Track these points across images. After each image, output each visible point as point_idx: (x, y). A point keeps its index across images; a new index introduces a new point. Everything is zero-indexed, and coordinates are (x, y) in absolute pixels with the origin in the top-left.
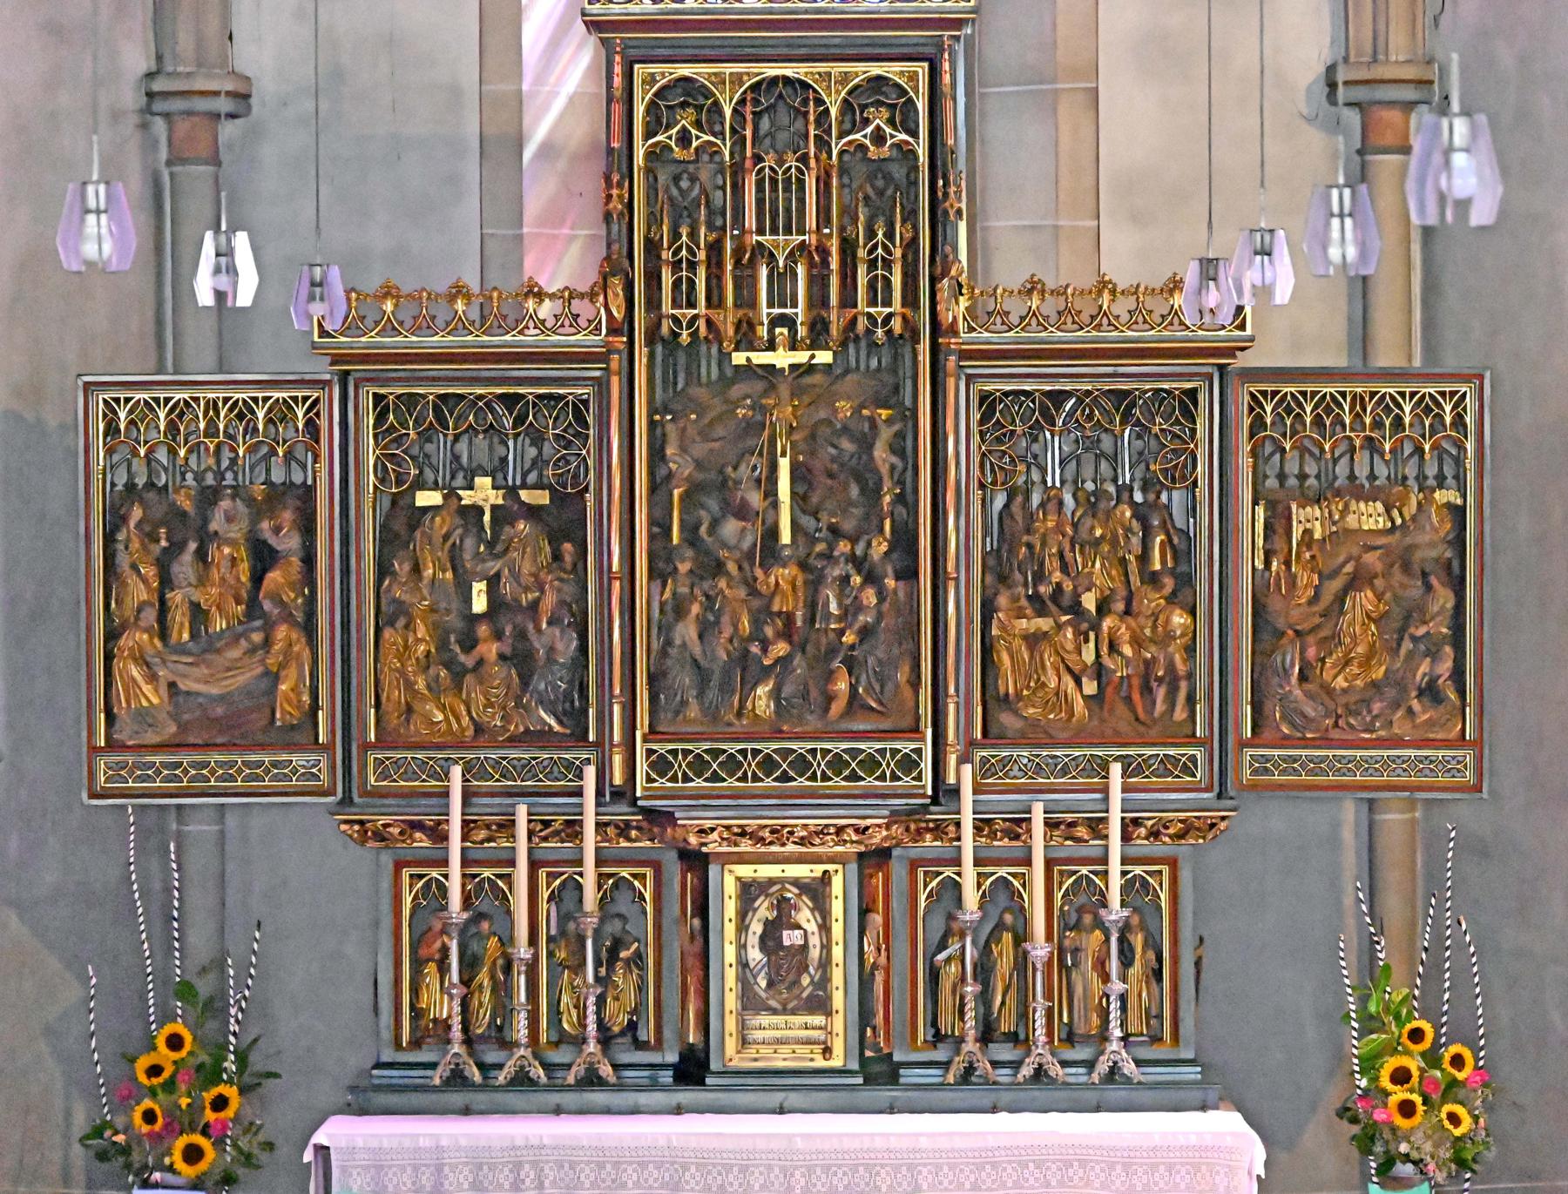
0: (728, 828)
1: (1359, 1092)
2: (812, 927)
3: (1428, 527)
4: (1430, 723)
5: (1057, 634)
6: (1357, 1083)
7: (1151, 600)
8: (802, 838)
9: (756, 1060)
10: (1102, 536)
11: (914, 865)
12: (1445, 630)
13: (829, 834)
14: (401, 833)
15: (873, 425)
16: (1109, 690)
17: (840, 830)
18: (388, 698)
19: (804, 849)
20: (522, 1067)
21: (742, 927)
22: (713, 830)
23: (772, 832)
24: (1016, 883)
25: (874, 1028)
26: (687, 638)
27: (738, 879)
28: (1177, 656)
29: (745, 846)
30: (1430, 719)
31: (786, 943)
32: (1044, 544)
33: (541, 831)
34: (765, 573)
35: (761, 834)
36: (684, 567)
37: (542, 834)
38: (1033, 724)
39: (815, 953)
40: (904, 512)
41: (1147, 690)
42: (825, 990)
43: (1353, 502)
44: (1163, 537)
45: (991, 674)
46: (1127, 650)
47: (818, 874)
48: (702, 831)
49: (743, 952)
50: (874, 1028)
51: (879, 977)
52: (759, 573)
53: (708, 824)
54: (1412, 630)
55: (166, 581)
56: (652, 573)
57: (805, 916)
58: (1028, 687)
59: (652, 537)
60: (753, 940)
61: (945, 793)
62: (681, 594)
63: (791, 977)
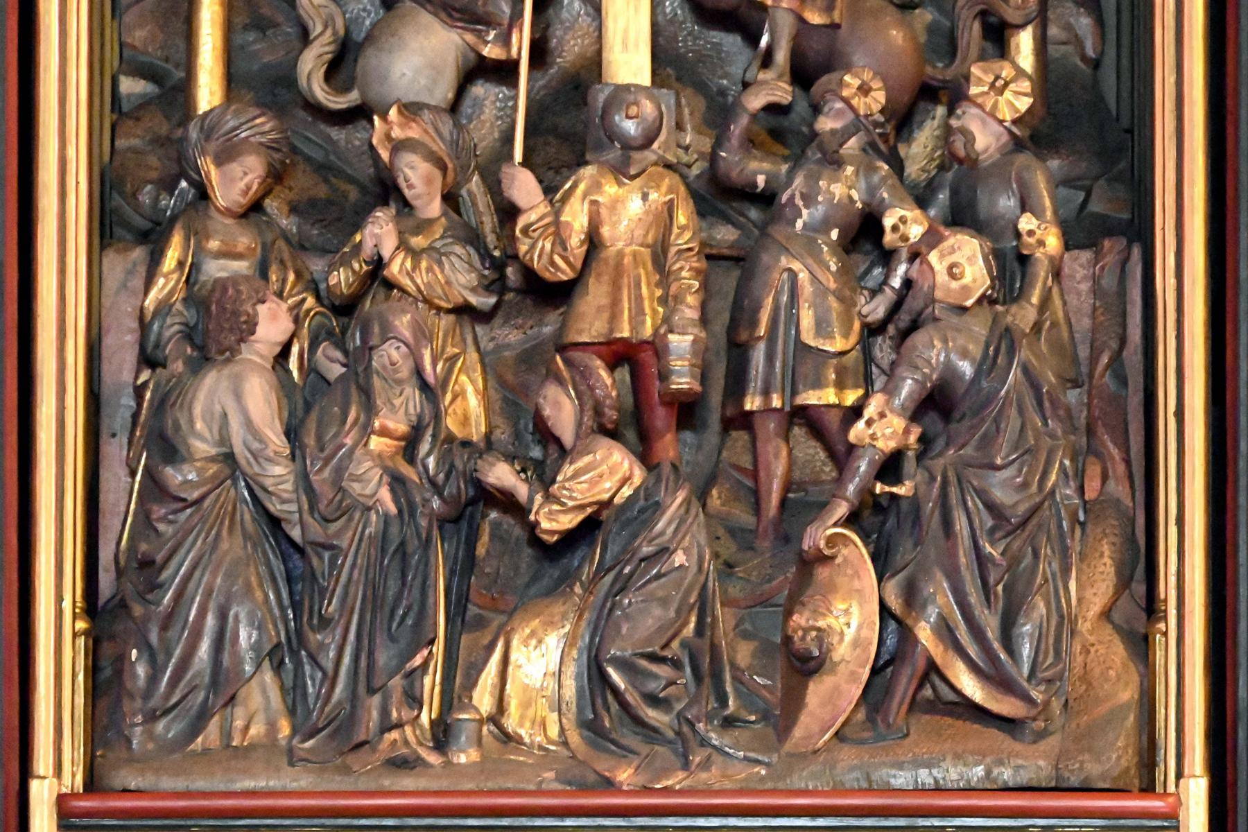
34: (549, 190)
62: (221, 285)
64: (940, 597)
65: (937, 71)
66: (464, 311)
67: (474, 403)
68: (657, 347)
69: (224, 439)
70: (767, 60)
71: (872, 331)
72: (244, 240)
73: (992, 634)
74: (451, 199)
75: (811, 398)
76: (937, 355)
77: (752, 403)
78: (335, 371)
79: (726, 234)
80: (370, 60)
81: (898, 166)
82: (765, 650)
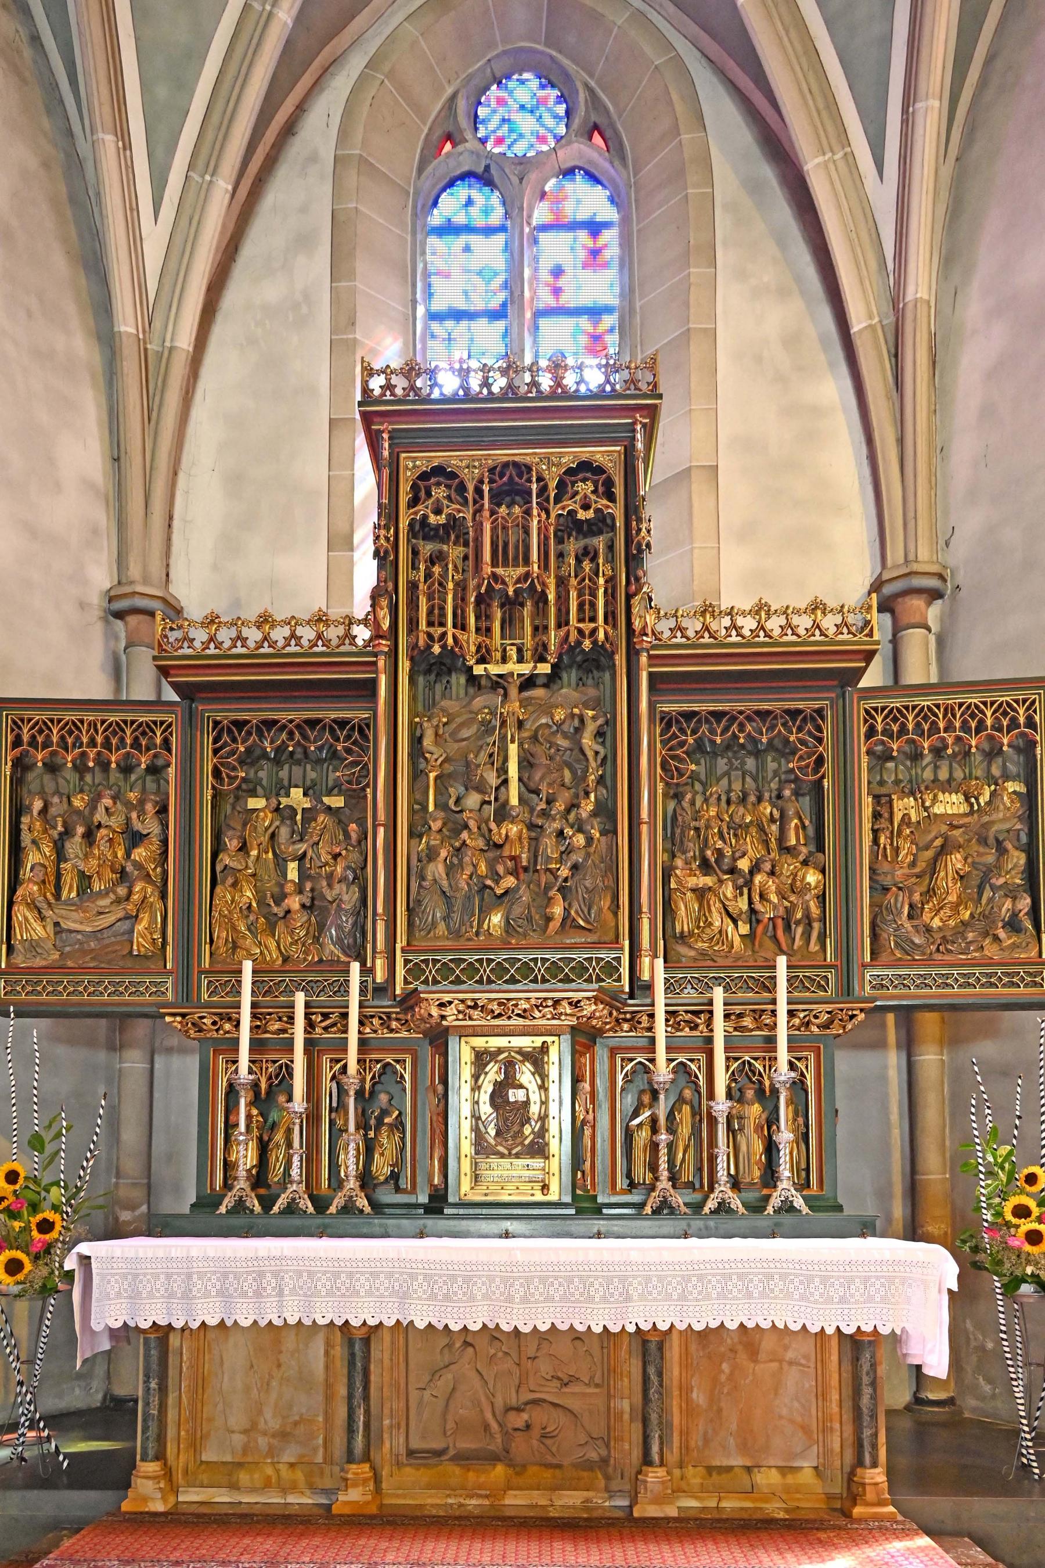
0: (463, 1001)
1: (986, 1224)
2: (533, 1087)
3: (1002, 807)
4: (1014, 946)
5: (720, 887)
6: (985, 1217)
7: (788, 867)
8: (525, 1011)
9: (486, 1195)
10: (751, 821)
11: (613, 1052)
12: (1018, 881)
13: (547, 1006)
14: (214, 1023)
15: (582, 720)
16: (760, 929)
17: (557, 1002)
18: (218, 937)
19: (528, 1022)
20: (294, 1199)
21: (476, 1088)
22: (450, 1003)
23: (500, 1004)
24: (693, 1067)
25: (583, 1172)
26: (437, 875)
27: (473, 1048)
28: (812, 904)
29: (479, 1019)
30: (1013, 943)
31: (512, 1099)
32: (708, 827)
33: (321, 1021)
34: (498, 826)
35: (490, 1007)
36: (436, 826)
37: (323, 1024)
38: (703, 954)
39: (535, 1109)
40: (605, 791)
41: (788, 928)
42: (543, 1138)
43: (940, 794)
44: (796, 821)
45: (669, 918)
46: (774, 898)
47: (539, 1044)
48: (442, 1005)
49: (476, 1107)
50: (583, 1172)
51: (587, 1132)
52: (493, 826)
53: (447, 997)
54: (993, 881)
55: (60, 855)
56: (411, 834)
57: (526, 1075)
58: (698, 927)
59: (412, 812)
60: (485, 1097)
61: (640, 988)
62: (433, 846)
63: (516, 1128)
64: (576, 905)
65: (575, 801)
66: (481, 850)
67: (483, 868)
68: (519, 857)
69: (434, 876)
70: (541, 800)
71: (562, 853)
72: (438, 837)
73: (586, 912)
74: (479, 828)
75: (550, 866)
76: (575, 857)
77: (538, 868)
78: (456, 862)
79: (533, 834)
80: (463, 801)
81: (567, 820)
82: (541, 917)
